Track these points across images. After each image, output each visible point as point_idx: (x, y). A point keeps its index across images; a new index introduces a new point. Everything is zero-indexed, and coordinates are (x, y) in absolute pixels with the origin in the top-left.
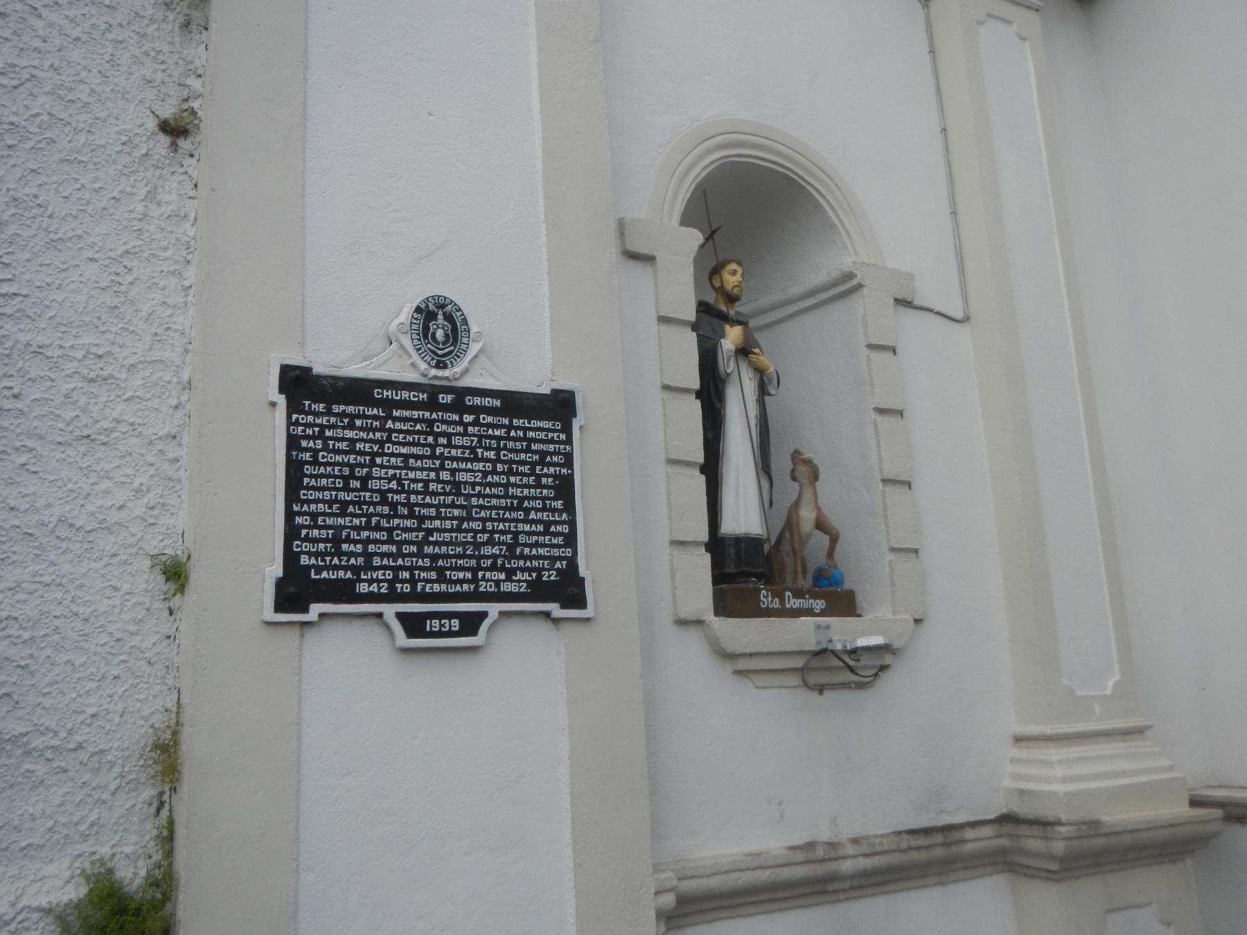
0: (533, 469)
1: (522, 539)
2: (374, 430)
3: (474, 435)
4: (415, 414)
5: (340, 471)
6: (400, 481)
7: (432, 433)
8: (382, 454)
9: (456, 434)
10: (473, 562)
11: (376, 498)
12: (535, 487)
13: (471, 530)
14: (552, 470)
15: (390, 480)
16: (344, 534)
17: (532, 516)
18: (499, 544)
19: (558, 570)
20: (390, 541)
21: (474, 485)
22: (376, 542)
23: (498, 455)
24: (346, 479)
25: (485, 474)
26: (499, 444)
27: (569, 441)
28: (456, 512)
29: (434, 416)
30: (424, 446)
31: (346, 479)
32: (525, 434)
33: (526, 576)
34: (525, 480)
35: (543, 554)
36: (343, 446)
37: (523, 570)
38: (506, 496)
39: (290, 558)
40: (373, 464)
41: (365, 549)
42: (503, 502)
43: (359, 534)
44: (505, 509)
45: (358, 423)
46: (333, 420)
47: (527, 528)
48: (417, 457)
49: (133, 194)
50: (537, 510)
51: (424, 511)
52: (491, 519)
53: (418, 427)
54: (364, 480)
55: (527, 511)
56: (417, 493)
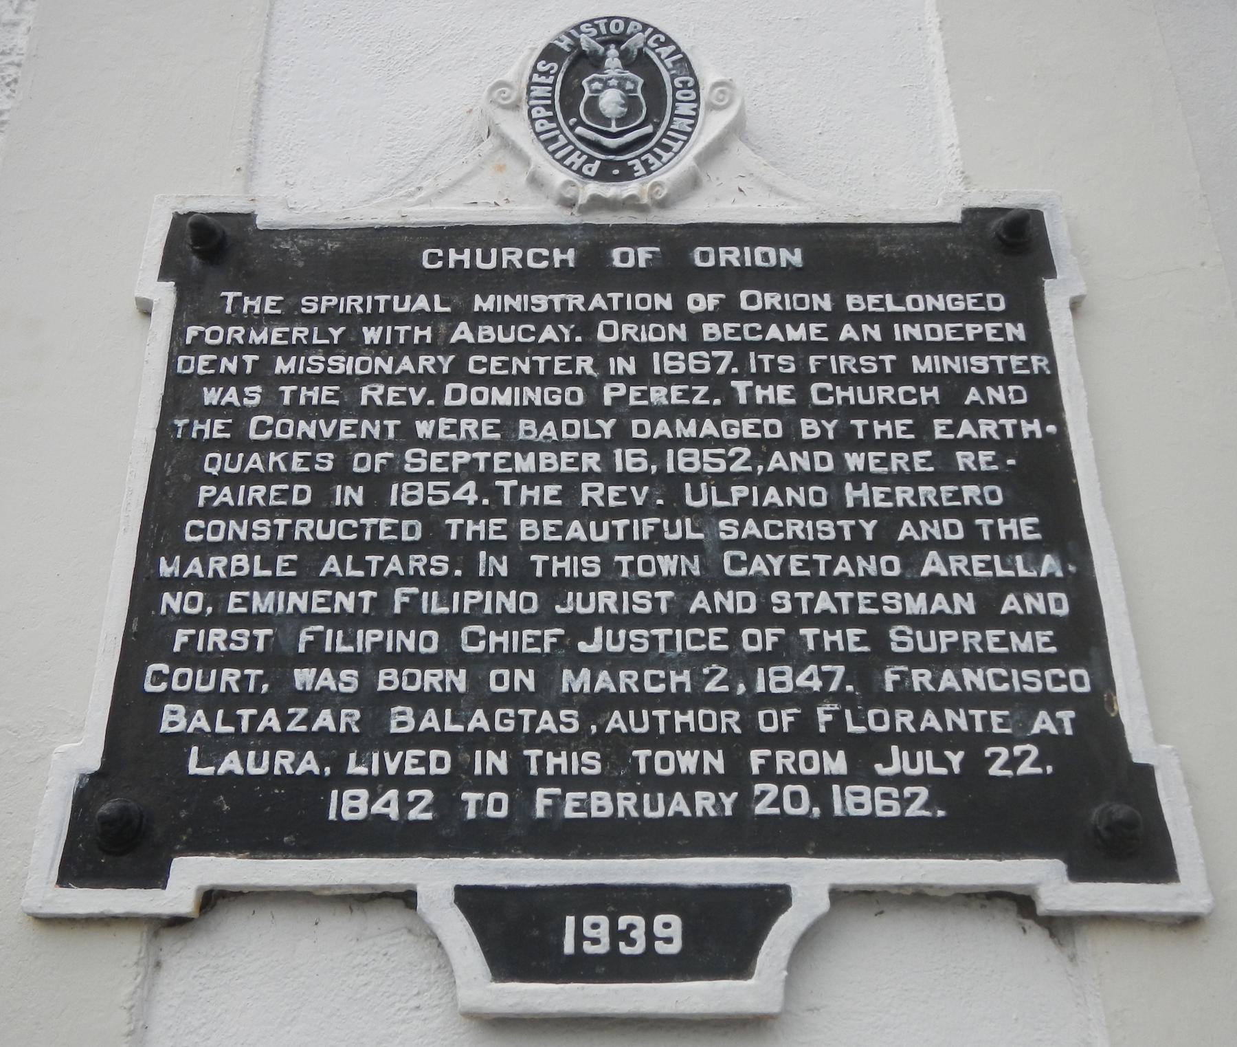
0: (922, 431)
1: (900, 639)
2: (413, 351)
3: (722, 345)
4: (541, 302)
5: (308, 461)
6: (486, 483)
7: (590, 346)
8: (440, 411)
9: (662, 347)
10: (731, 719)
11: (411, 530)
12: (933, 480)
13: (722, 617)
14: (988, 427)
15: (456, 481)
16: (304, 637)
17: (932, 565)
18: (820, 656)
19: (1042, 739)
20: (450, 657)
21: (724, 482)
22: (402, 659)
23: (801, 393)
24: (322, 483)
25: (761, 449)
26: (802, 364)
27: (1039, 340)
28: (668, 564)
29: (598, 301)
30: (563, 381)
31: (322, 483)
32: (887, 332)
33: (926, 762)
34: (898, 461)
36: (322, 395)
37: (912, 742)
38: (835, 510)
39: (131, 710)
40: (407, 436)
41: (367, 683)
42: (827, 529)
43: (350, 639)
44: (836, 547)
45: (371, 335)
46: (299, 332)
47: (917, 605)
48: (541, 414)
49: (15, 24)
50: (946, 548)
51: (564, 565)
52: (786, 581)
53: (549, 333)
54: (376, 485)
55: (913, 552)
56: (539, 512)
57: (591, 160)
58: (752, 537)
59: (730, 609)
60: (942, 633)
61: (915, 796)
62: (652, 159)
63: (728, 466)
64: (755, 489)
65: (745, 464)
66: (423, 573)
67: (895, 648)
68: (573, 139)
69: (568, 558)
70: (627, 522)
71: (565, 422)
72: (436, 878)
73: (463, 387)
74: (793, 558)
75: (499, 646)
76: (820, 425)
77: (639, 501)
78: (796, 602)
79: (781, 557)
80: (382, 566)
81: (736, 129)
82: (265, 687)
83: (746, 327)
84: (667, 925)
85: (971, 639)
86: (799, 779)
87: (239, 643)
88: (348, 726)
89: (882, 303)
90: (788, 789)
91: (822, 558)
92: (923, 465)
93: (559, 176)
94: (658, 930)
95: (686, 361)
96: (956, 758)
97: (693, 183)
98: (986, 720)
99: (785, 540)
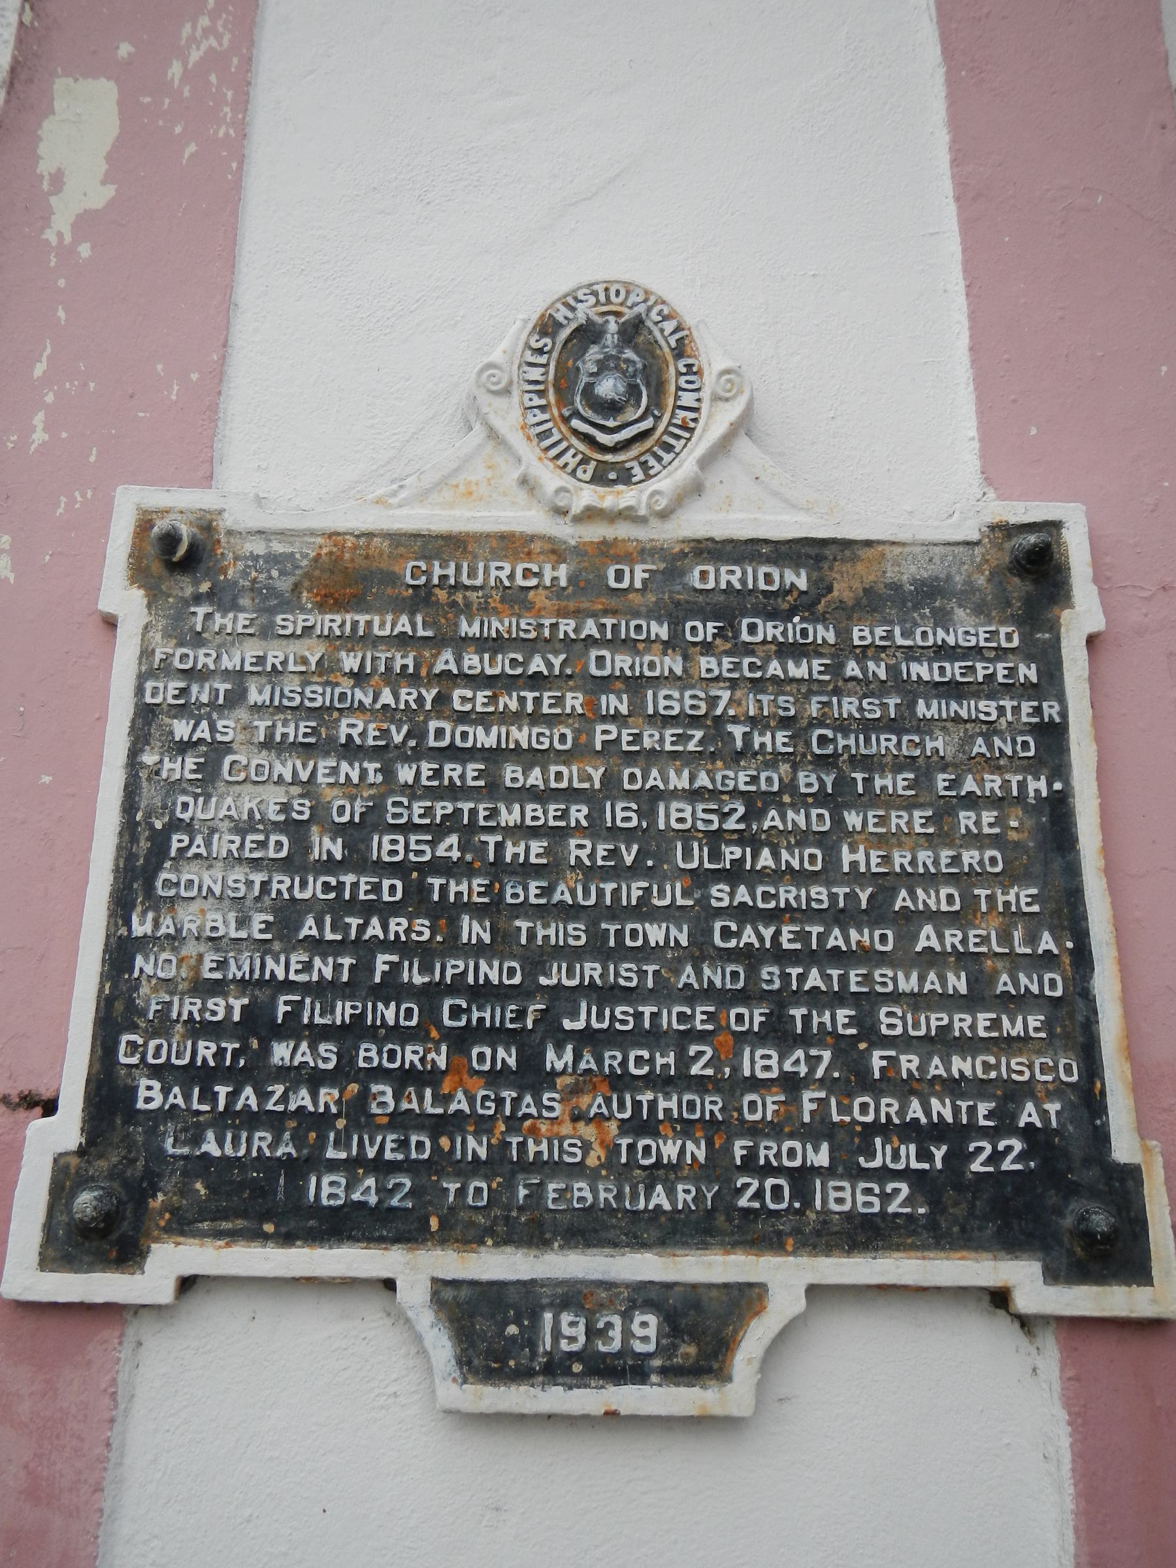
1: (889, 1020)
10: (713, 1105)
11: (392, 889)
15: (439, 831)
17: (927, 937)
21: (715, 839)
25: (756, 803)
29: (590, 628)
30: (551, 720)
35: (958, 1060)
38: (829, 874)
41: (346, 1058)
43: (328, 1010)
47: (908, 983)
48: (530, 757)
51: (550, 932)
52: (780, 956)
55: (909, 920)
56: (526, 870)
57: (585, 461)
58: (743, 904)
59: (718, 984)
60: (933, 1016)
61: (897, 1191)
62: (652, 462)
63: (720, 823)
64: (748, 850)
65: (738, 821)
66: (403, 938)
67: (884, 1031)
68: (568, 434)
69: (553, 925)
70: (615, 885)
71: (553, 769)
72: (415, 1269)
73: (447, 726)
74: (785, 929)
75: (481, 1020)
76: (820, 779)
77: (629, 860)
78: (785, 977)
79: (772, 929)
80: (362, 929)
81: (743, 426)
82: (242, 1062)
83: (746, 661)
84: (644, 1324)
85: (961, 1023)
86: (779, 1171)
87: (214, 1013)
88: (327, 1105)
89: (889, 636)
90: (770, 1182)
91: (816, 930)
92: (923, 825)
93: (551, 479)
94: (635, 1328)
95: (681, 700)
96: (939, 1153)
97: (695, 489)
98: (972, 1110)
99: (777, 908)
